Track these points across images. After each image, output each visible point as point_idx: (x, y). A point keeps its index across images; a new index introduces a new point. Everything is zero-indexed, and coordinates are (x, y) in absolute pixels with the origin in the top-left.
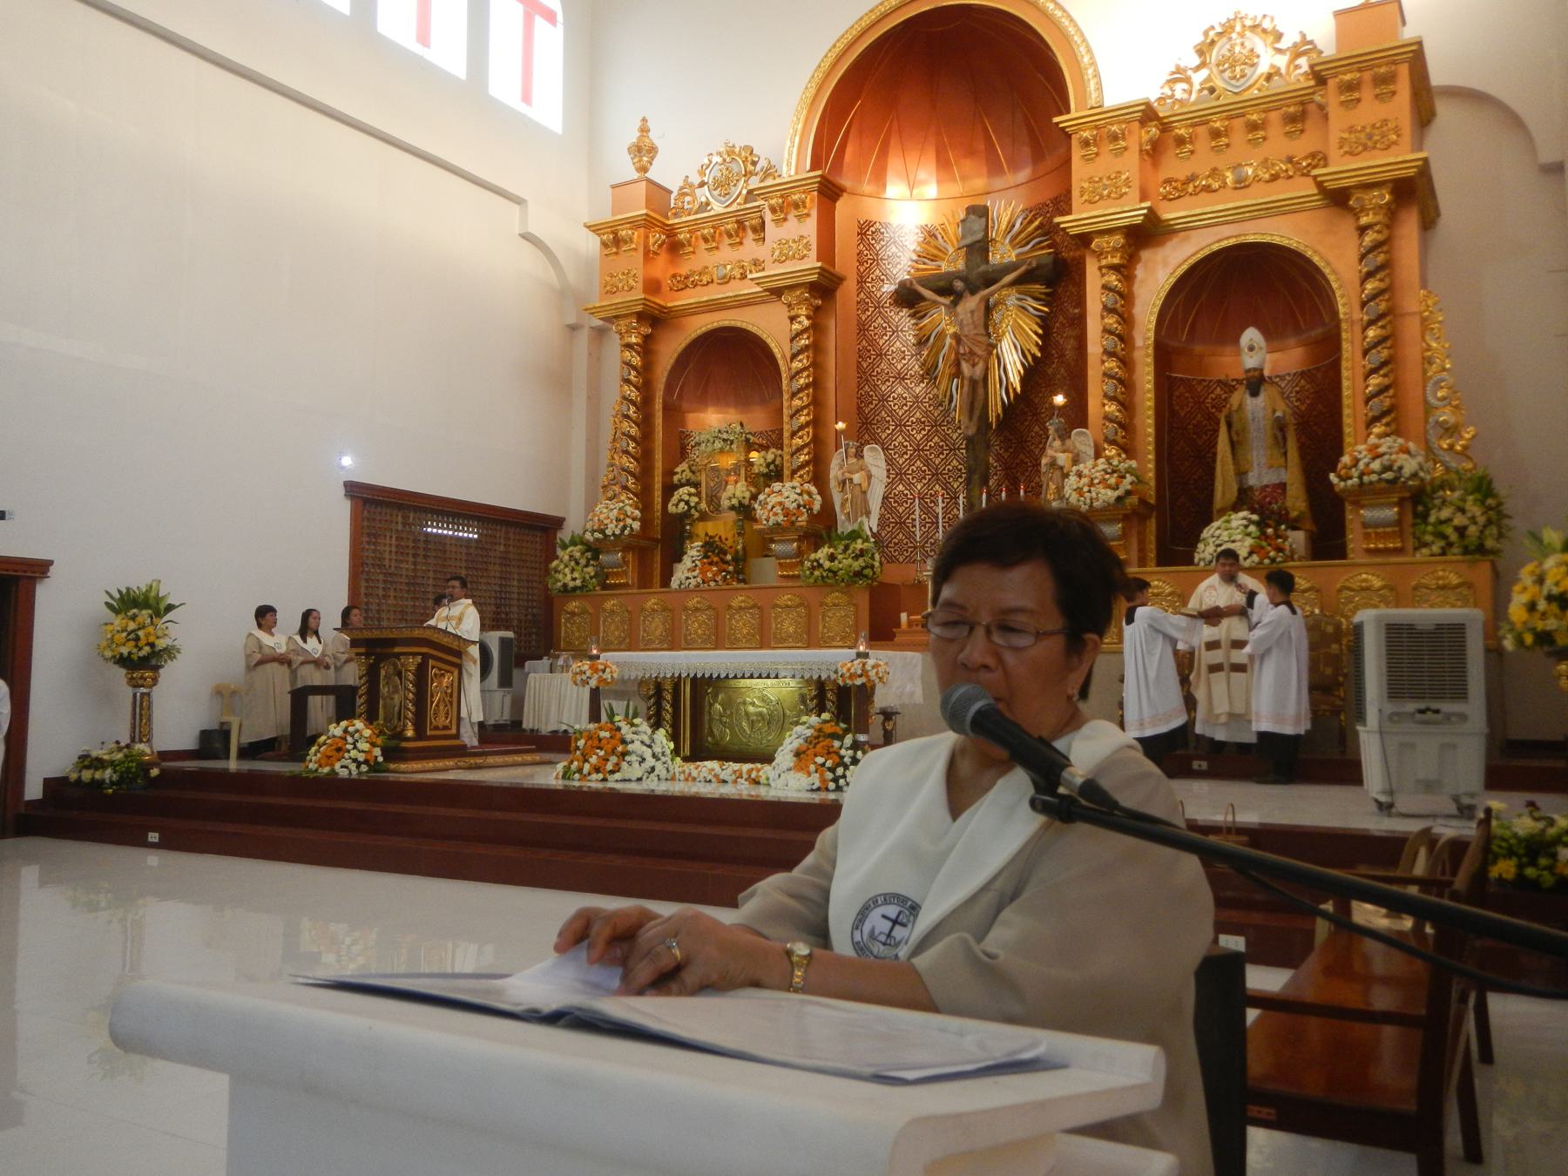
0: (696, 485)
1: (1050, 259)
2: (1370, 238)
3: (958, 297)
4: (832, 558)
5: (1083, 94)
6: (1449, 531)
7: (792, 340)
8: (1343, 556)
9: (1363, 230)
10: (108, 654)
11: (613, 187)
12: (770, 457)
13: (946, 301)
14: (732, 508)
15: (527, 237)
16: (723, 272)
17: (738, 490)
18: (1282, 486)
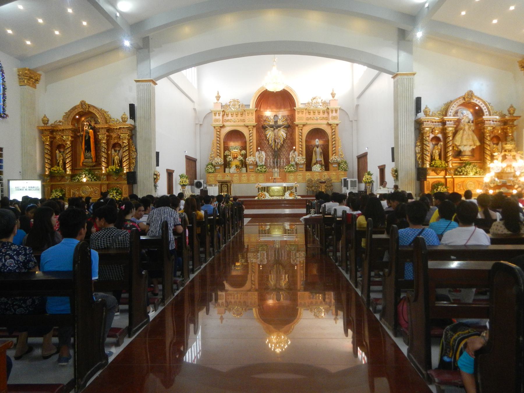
0: (230, 155)
1: (288, 125)
2: (334, 130)
3: (274, 129)
4: (261, 169)
5: (298, 105)
6: (343, 168)
7: (250, 134)
8: (329, 170)
9: (333, 129)
10: (182, 184)
11: (214, 103)
12: (244, 152)
13: (272, 129)
14: (240, 160)
15: (195, 109)
16: (235, 120)
17: (240, 158)
18: (321, 161)
